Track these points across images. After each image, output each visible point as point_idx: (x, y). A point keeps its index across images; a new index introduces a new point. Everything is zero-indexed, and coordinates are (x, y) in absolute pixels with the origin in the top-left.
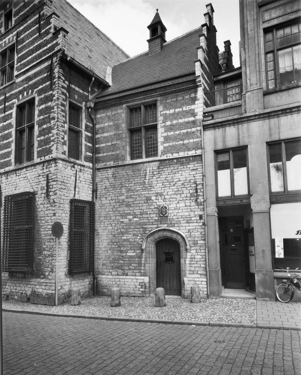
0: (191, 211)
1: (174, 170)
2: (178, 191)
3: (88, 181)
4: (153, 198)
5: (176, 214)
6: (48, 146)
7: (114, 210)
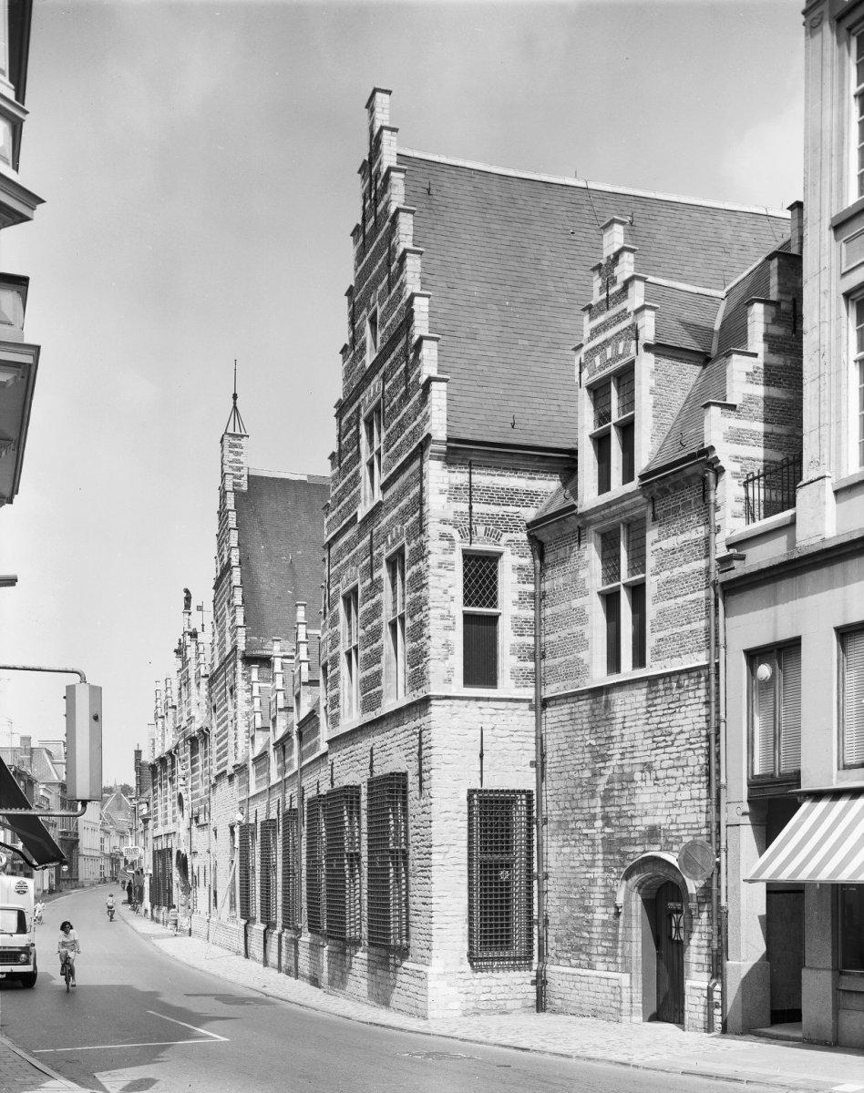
0: (701, 811)
1: (672, 702)
2: (678, 758)
3: (519, 733)
4: (638, 776)
5: (674, 817)
6: (420, 666)
7: (574, 804)
